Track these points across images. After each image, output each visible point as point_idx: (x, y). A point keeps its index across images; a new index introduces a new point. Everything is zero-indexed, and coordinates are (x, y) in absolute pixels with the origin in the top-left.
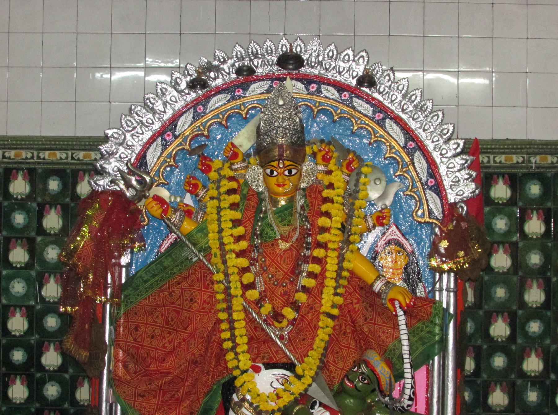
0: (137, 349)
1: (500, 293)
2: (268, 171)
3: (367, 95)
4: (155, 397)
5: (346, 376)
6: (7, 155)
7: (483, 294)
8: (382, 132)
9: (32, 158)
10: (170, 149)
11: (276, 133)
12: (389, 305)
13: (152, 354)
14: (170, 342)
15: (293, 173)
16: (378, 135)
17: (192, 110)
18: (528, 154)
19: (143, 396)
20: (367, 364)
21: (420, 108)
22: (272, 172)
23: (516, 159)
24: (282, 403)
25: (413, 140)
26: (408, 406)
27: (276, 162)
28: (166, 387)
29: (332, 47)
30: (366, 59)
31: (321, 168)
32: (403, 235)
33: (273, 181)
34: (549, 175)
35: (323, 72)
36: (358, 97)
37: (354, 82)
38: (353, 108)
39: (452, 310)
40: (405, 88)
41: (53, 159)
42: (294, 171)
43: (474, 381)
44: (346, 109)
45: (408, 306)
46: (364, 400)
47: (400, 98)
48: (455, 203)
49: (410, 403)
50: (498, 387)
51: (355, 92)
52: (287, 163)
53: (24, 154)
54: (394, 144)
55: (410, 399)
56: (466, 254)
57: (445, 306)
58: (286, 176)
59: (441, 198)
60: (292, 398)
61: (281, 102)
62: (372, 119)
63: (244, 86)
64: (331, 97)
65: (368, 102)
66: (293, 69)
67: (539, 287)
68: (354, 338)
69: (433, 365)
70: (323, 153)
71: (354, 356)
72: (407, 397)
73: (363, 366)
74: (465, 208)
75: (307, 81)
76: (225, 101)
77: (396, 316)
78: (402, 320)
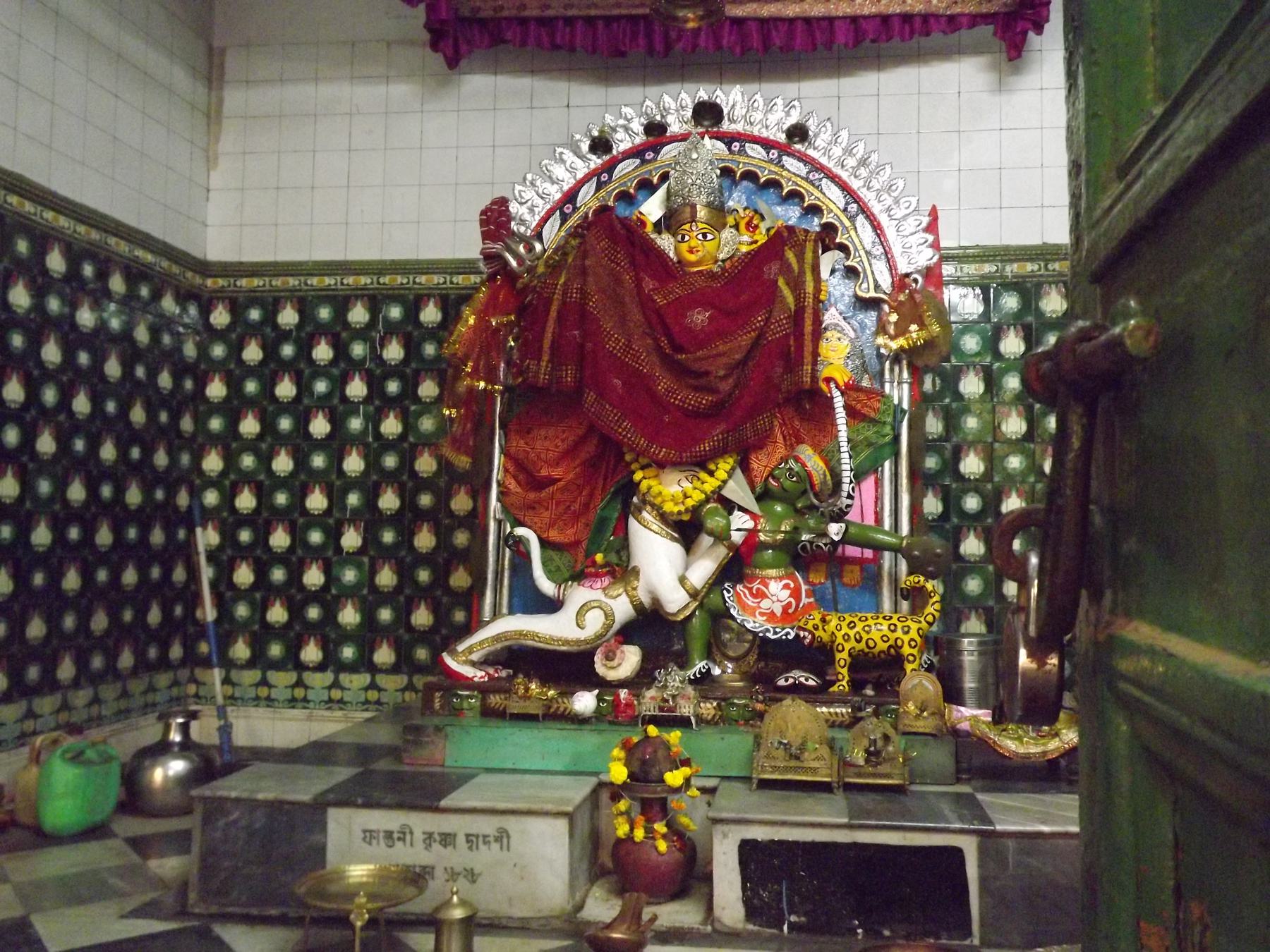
0: (528, 453)
1: (971, 423)
3: (799, 152)
4: (547, 509)
5: (771, 475)
6: (417, 280)
7: (952, 421)
9: (445, 283)
10: (570, 223)
12: (823, 386)
13: (543, 456)
14: (563, 441)
17: (595, 179)
18: (1002, 261)
19: (534, 508)
20: (797, 459)
21: (863, 162)
23: (988, 268)
24: (690, 503)
25: (856, 202)
26: (848, 506)
28: (558, 495)
29: (757, 97)
30: (798, 109)
31: (746, 238)
32: (845, 319)
33: (684, 247)
34: (1029, 285)
35: (748, 127)
36: (789, 155)
37: (782, 138)
38: (783, 166)
39: (905, 406)
40: (845, 141)
41: (467, 283)
42: (710, 237)
43: (942, 527)
44: (773, 168)
45: (846, 385)
46: (793, 505)
47: (837, 151)
48: (907, 275)
49: (849, 502)
50: (972, 533)
51: (784, 150)
52: (701, 225)
53: (437, 279)
54: (832, 206)
55: (850, 497)
56: (920, 330)
57: (896, 402)
59: (891, 270)
60: (703, 496)
62: (806, 179)
63: (656, 148)
65: (800, 160)
66: (712, 126)
67: (1019, 415)
68: (782, 433)
69: (882, 471)
70: (747, 219)
71: (781, 451)
72: (845, 494)
73: (791, 462)
74: (920, 280)
75: (728, 139)
77: (832, 398)
78: (839, 402)
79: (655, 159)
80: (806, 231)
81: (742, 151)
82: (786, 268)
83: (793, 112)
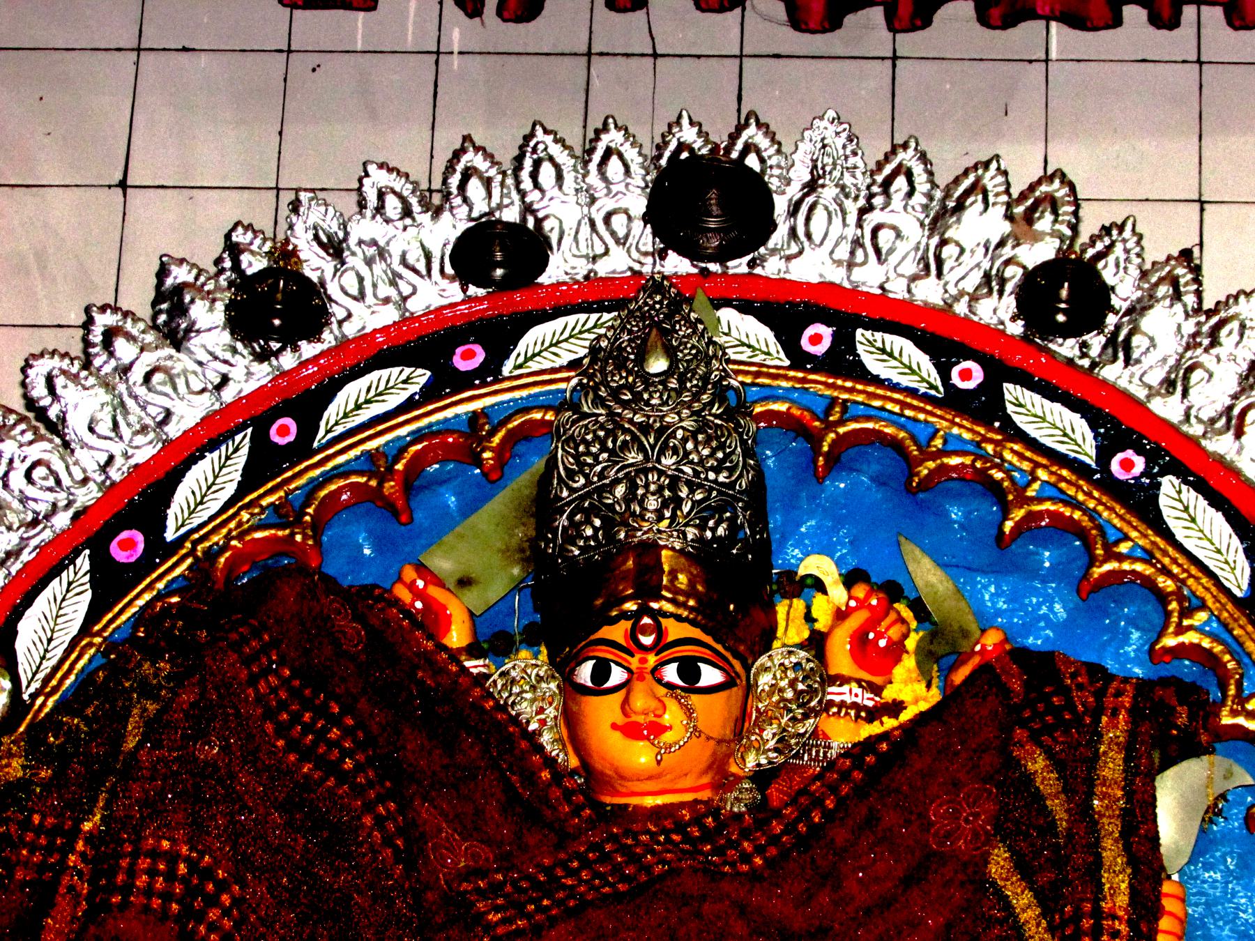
2: (585, 673)
8: (1140, 536)
11: (630, 497)
15: (702, 683)
16: (1124, 548)
17: (244, 440)
22: (602, 672)
27: (626, 625)
42: (710, 675)
58: (670, 686)
61: (658, 365)
64: (906, 381)
76: (402, 397)
79: (490, 371)
80: (1096, 670)
81: (842, 361)
82: (1020, 817)
83: (1044, 223)
